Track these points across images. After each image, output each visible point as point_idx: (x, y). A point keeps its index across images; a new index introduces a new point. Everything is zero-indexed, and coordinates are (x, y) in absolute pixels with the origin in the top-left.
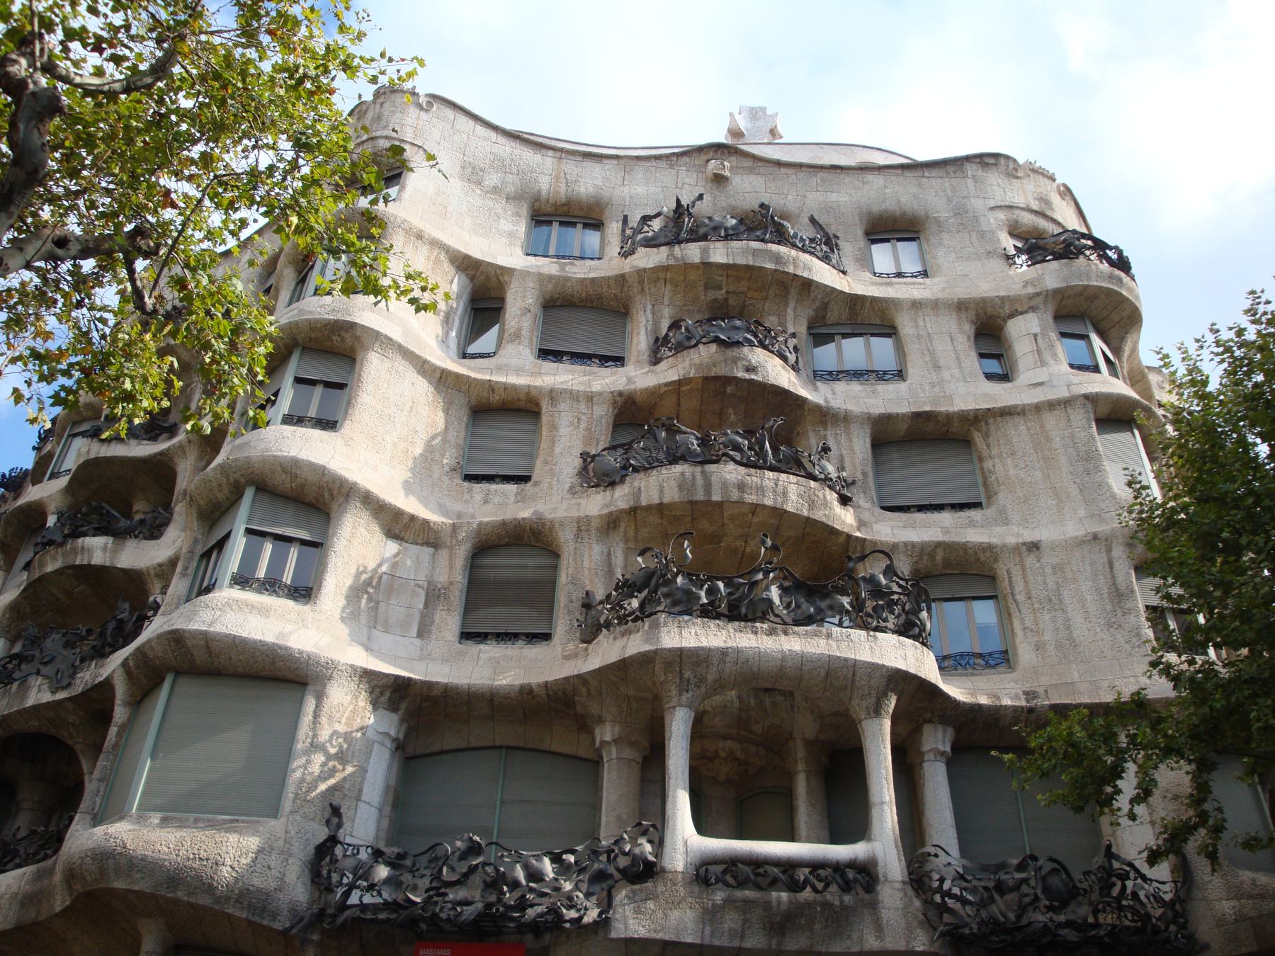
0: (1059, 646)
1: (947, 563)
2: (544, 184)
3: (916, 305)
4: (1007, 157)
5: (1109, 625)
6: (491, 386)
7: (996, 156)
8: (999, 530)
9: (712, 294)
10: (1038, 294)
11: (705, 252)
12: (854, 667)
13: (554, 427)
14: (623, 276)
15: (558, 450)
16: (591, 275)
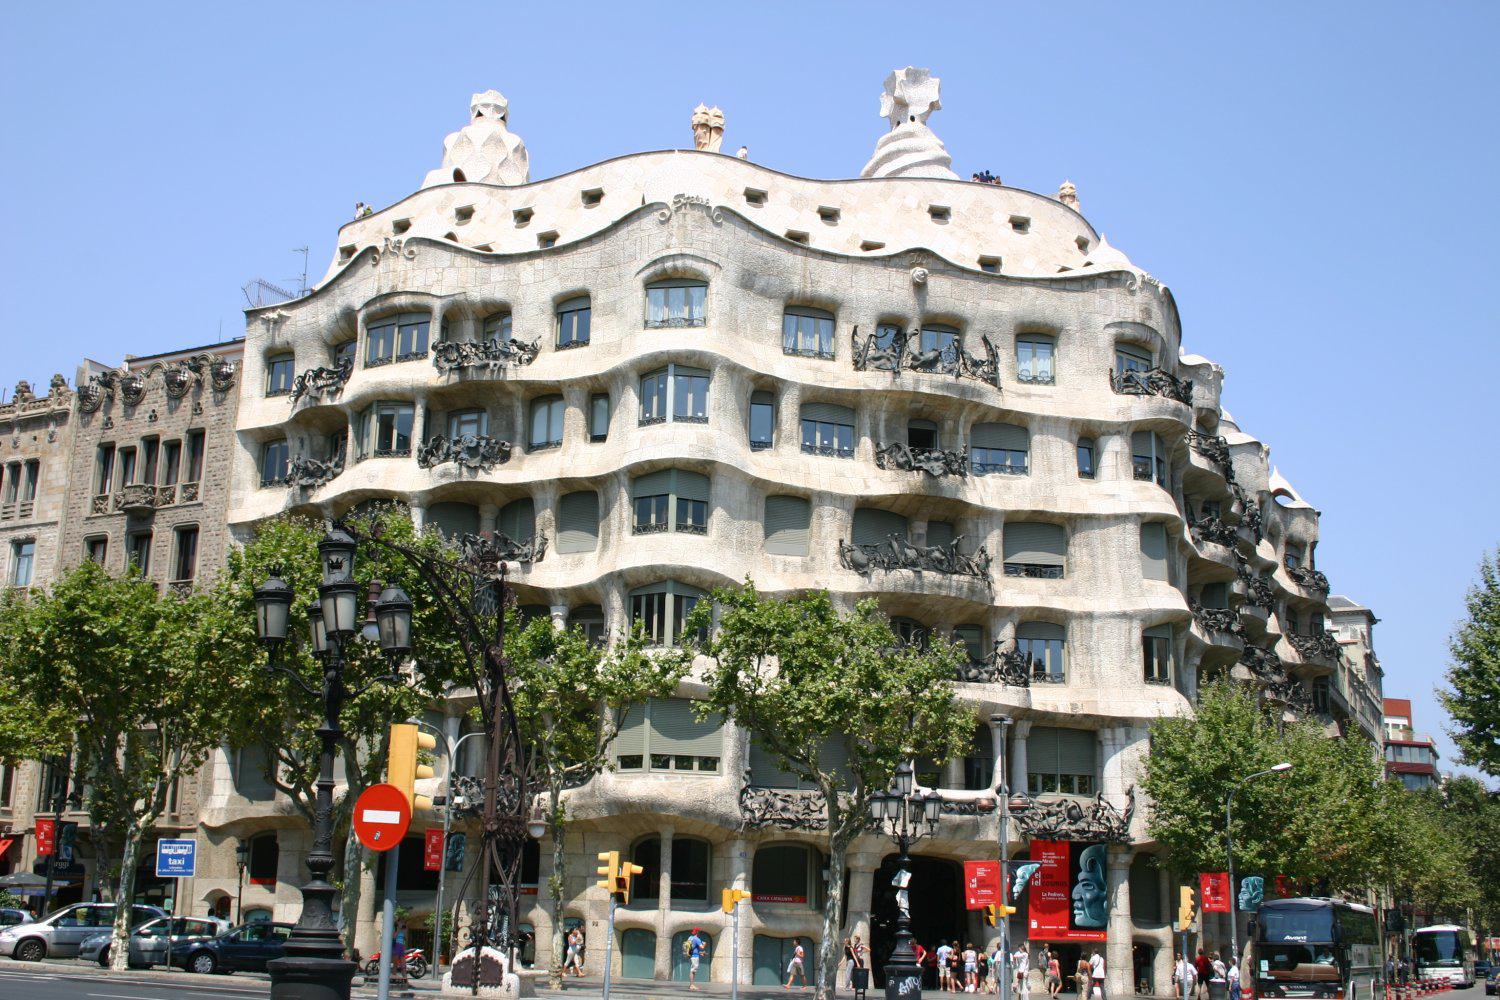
0: (1092, 677)
1: (1038, 617)
2: (797, 285)
3: (1044, 418)
4: (1128, 273)
5: (1122, 668)
6: (782, 486)
7: (1119, 273)
8: (1071, 599)
9: (914, 405)
10: (1125, 423)
11: (917, 381)
12: (995, 706)
13: (821, 517)
14: (859, 391)
15: (823, 534)
16: (838, 385)
